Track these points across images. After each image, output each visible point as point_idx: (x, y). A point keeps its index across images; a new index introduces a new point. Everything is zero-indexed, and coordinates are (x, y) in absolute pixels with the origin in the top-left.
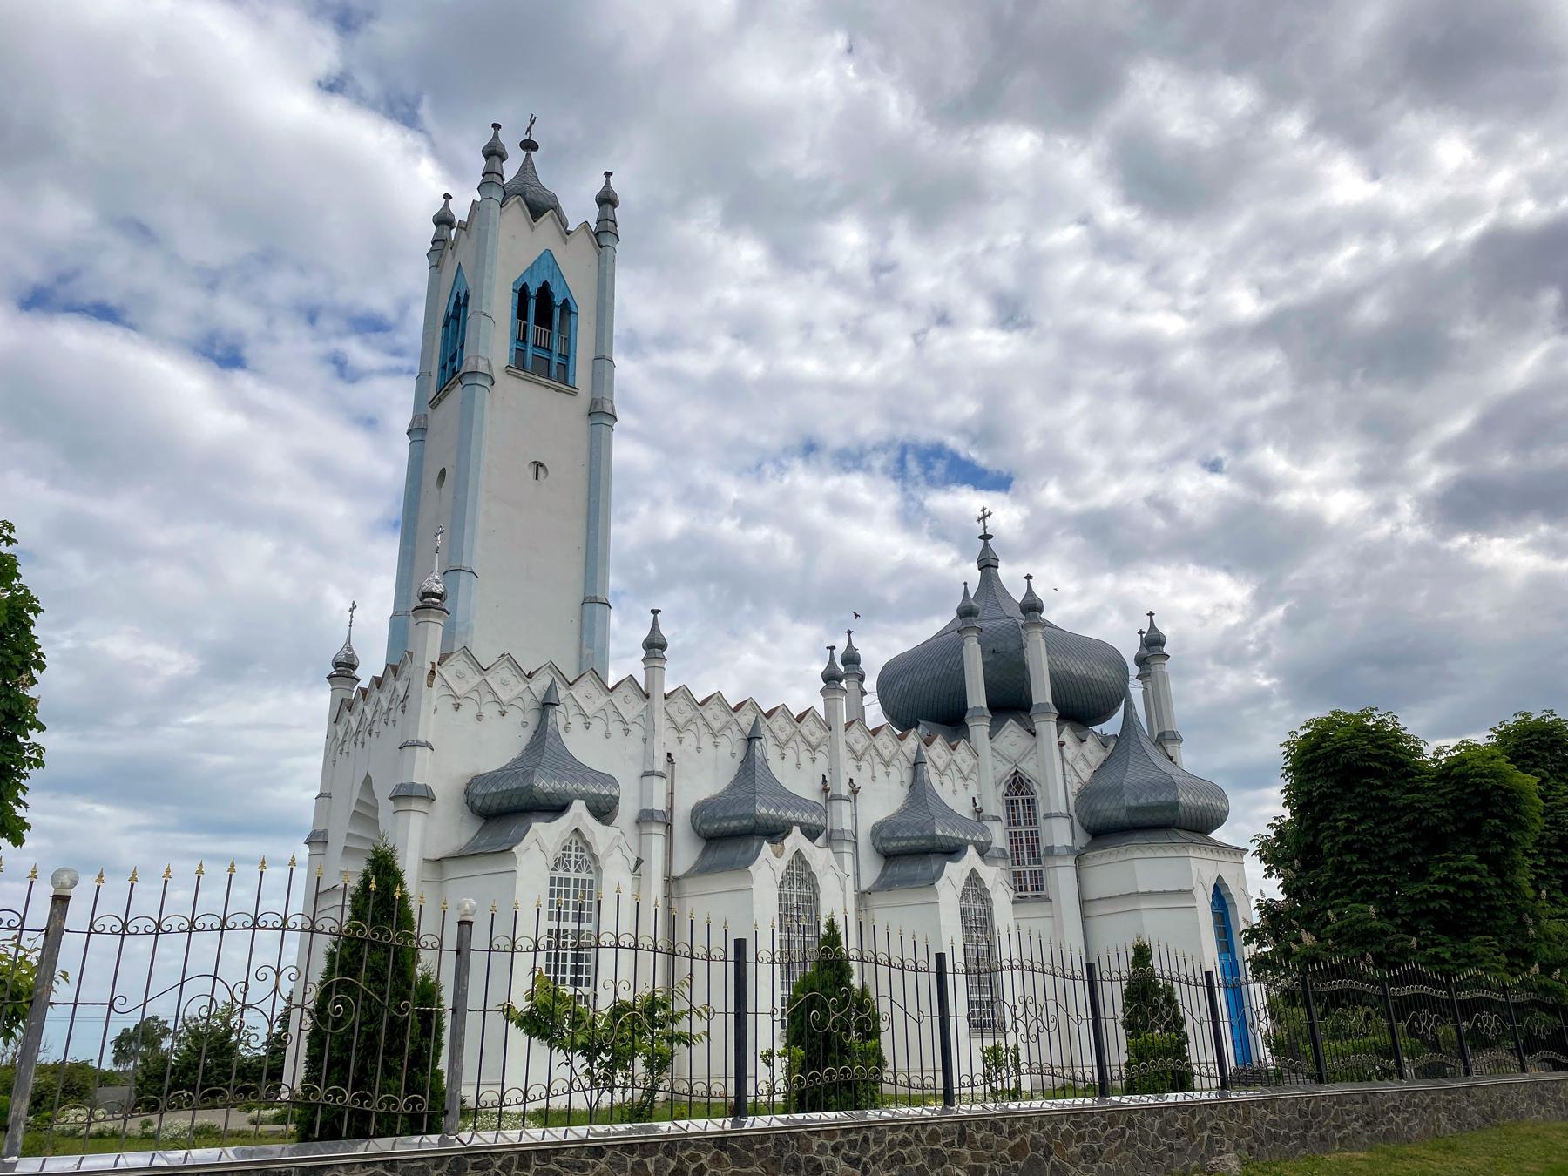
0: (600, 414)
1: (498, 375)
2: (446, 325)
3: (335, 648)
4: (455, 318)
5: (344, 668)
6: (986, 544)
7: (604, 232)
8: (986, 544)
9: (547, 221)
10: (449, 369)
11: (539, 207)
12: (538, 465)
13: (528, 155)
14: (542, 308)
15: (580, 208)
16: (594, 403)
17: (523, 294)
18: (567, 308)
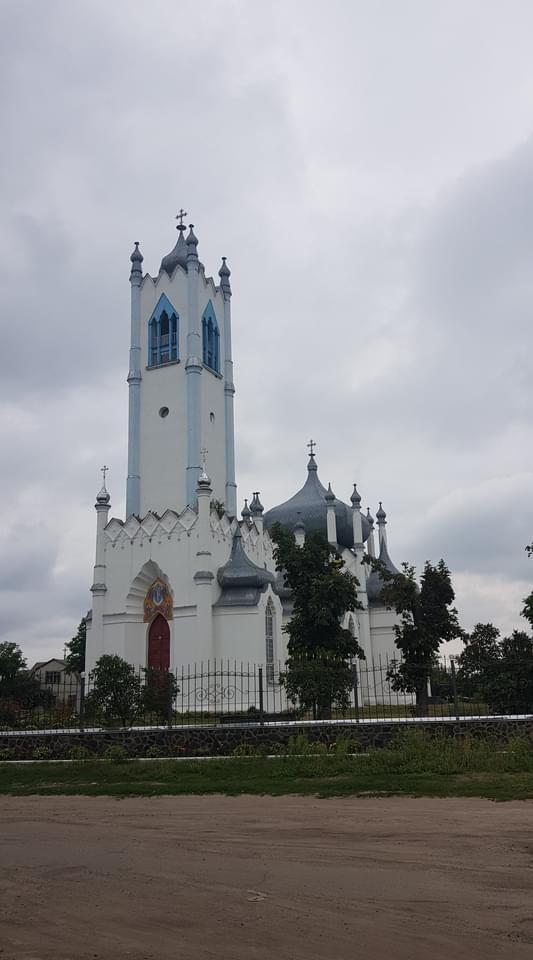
0: (229, 390)
2: (153, 323)
3: (97, 493)
5: (103, 503)
6: (312, 459)
7: (225, 290)
8: (312, 459)
12: (212, 414)
13: (181, 233)
16: (226, 384)
17: (204, 321)
18: (217, 334)
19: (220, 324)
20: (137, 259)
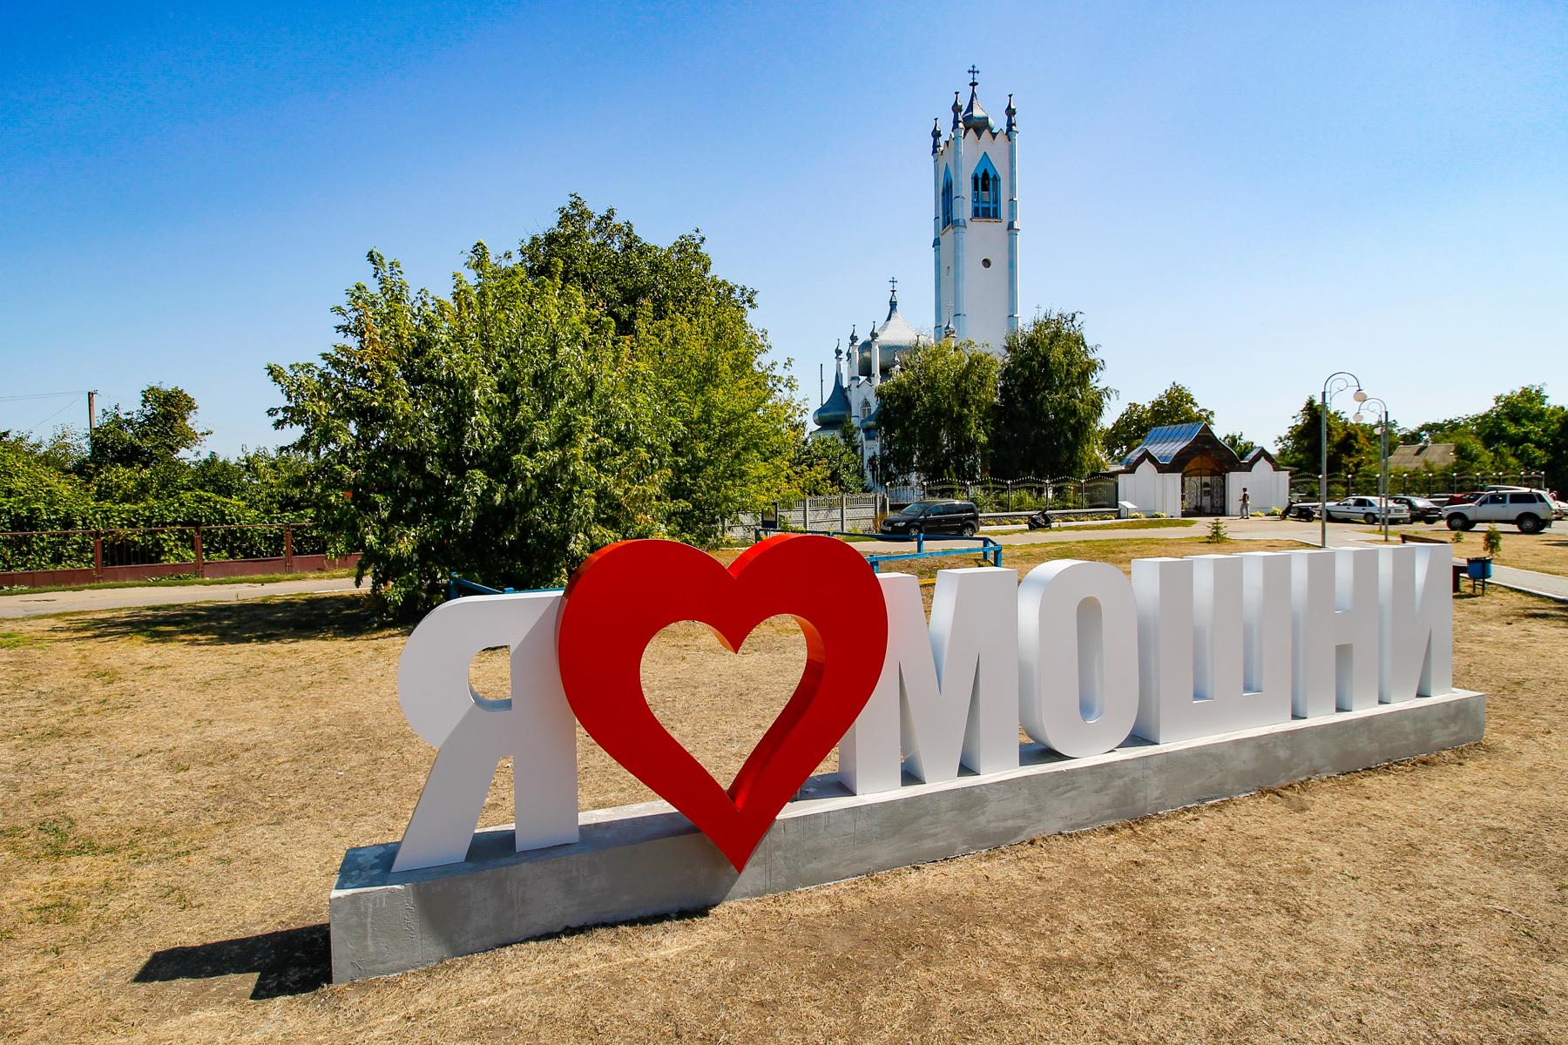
1: (968, 223)
4: (947, 194)
9: (986, 134)
10: (947, 218)
11: (979, 127)
14: (985, 181)
15: (998, 122)
17: (975, 179)
18: (996, 179)
19: (1000, 169)
20: (936, 134)
